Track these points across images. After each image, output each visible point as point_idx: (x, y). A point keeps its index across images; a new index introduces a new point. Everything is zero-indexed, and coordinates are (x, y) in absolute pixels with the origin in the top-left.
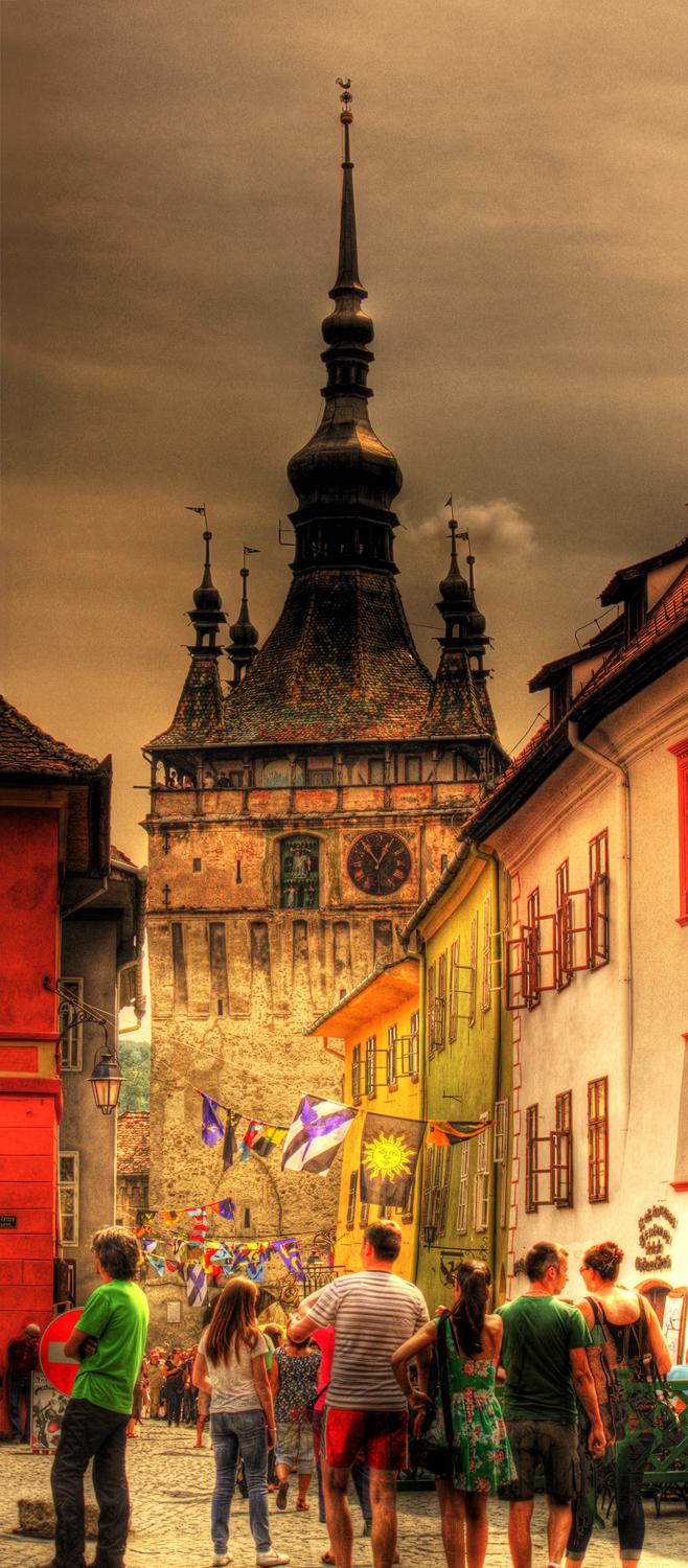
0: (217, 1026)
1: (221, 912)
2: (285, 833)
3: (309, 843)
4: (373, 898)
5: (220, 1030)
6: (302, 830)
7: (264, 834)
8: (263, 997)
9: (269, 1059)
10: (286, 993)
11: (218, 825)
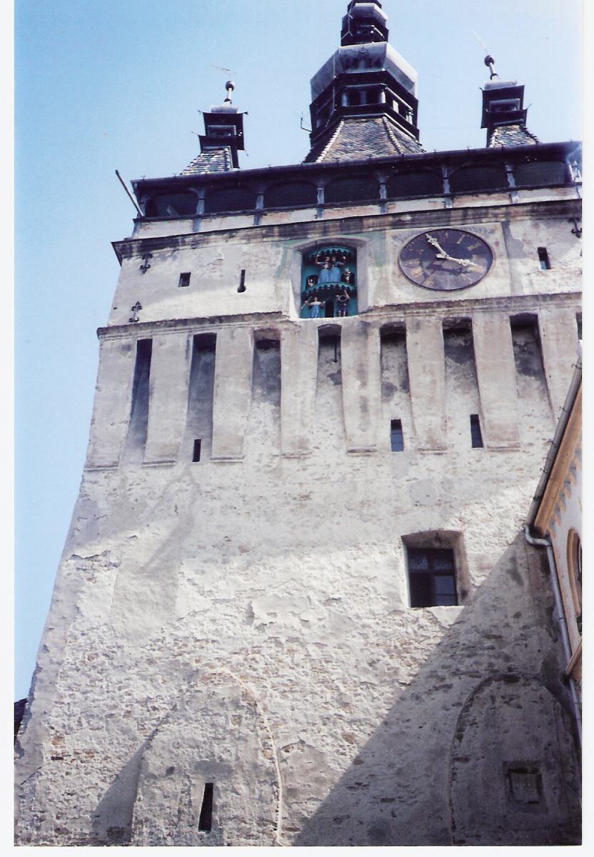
0: (189, 474)
1: (212, 320)
2: (311, 240)
3: (342, 250)
4: (440, 297)
5: (193, 481)
6: (334, 236)
7: (282, 245)
8: (266, 433)
9: (271, 516)
10: (303, 424)
11: (219, 237)
